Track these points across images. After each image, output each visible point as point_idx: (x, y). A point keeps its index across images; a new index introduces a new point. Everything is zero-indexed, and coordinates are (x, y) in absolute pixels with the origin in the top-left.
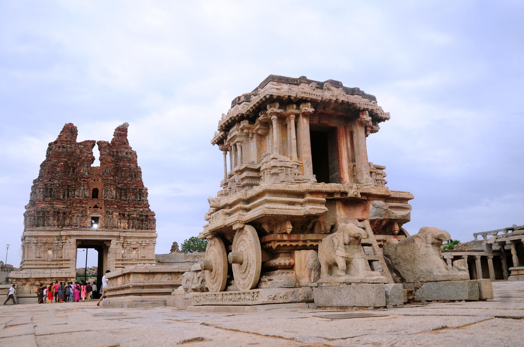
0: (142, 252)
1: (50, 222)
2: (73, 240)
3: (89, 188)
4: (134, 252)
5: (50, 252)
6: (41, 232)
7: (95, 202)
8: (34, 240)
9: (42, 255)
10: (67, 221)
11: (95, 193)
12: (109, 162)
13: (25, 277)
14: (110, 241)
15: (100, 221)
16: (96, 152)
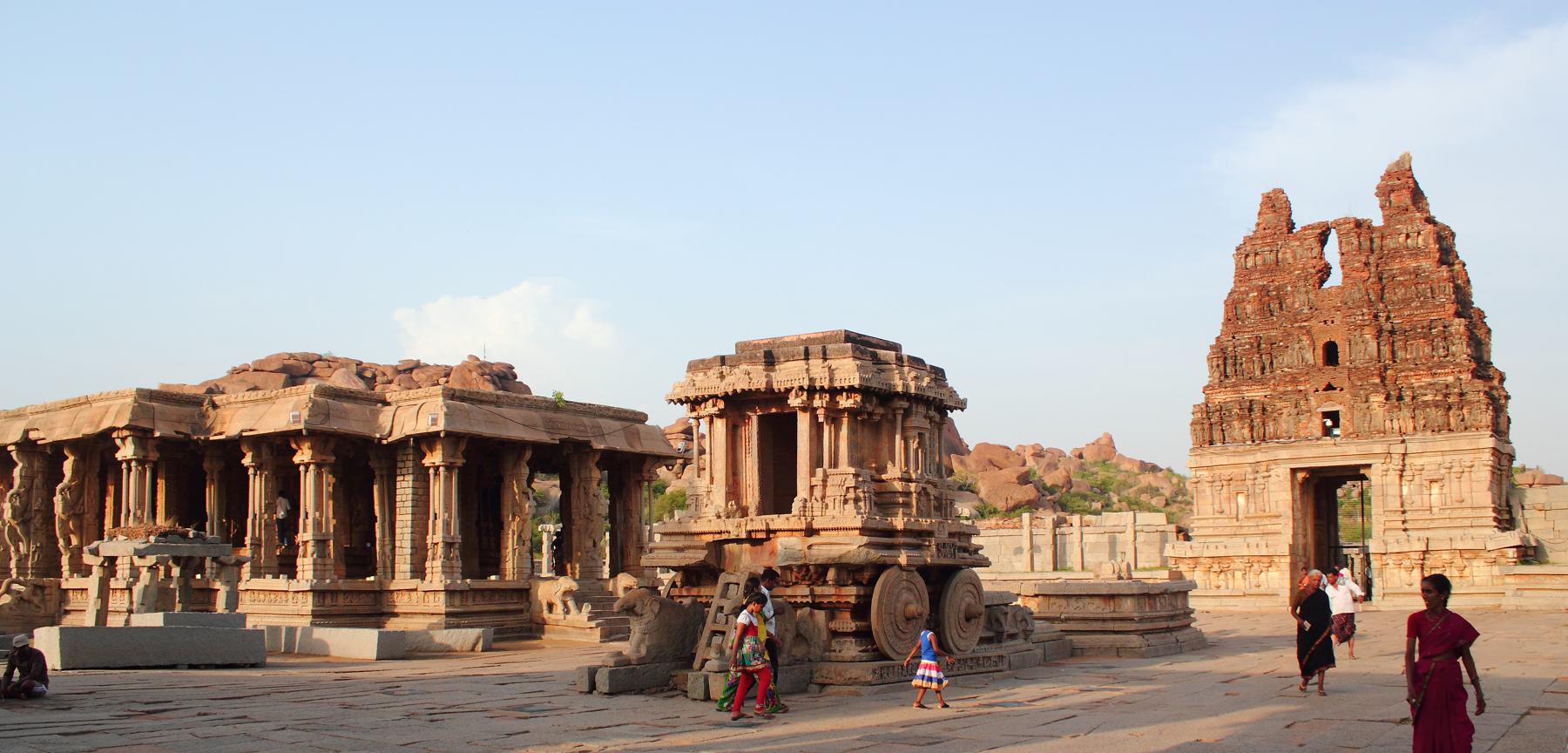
0: (1454, 488)
1: (1236, 433)
2: (1282, 472)
3: (1313, 343)
4: (1435, 488)
5: (1241, 499)
6: (1219, 458)
7: (1329, 374)
8: (1205, 474)
9: (1225, 507)
10: (1270, 428)
11: (1331, 354)
12: (1357, 270)
13: (1190, 554)
14: (1369, 466)
15: (1342, 421)
16: (1332, 252)
